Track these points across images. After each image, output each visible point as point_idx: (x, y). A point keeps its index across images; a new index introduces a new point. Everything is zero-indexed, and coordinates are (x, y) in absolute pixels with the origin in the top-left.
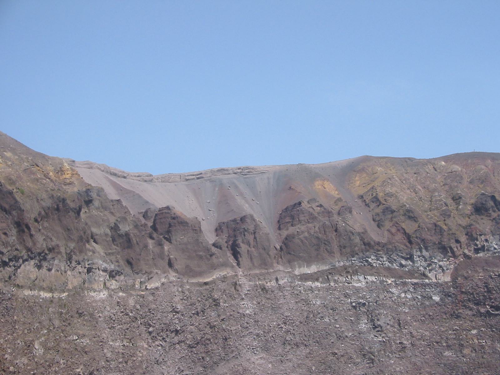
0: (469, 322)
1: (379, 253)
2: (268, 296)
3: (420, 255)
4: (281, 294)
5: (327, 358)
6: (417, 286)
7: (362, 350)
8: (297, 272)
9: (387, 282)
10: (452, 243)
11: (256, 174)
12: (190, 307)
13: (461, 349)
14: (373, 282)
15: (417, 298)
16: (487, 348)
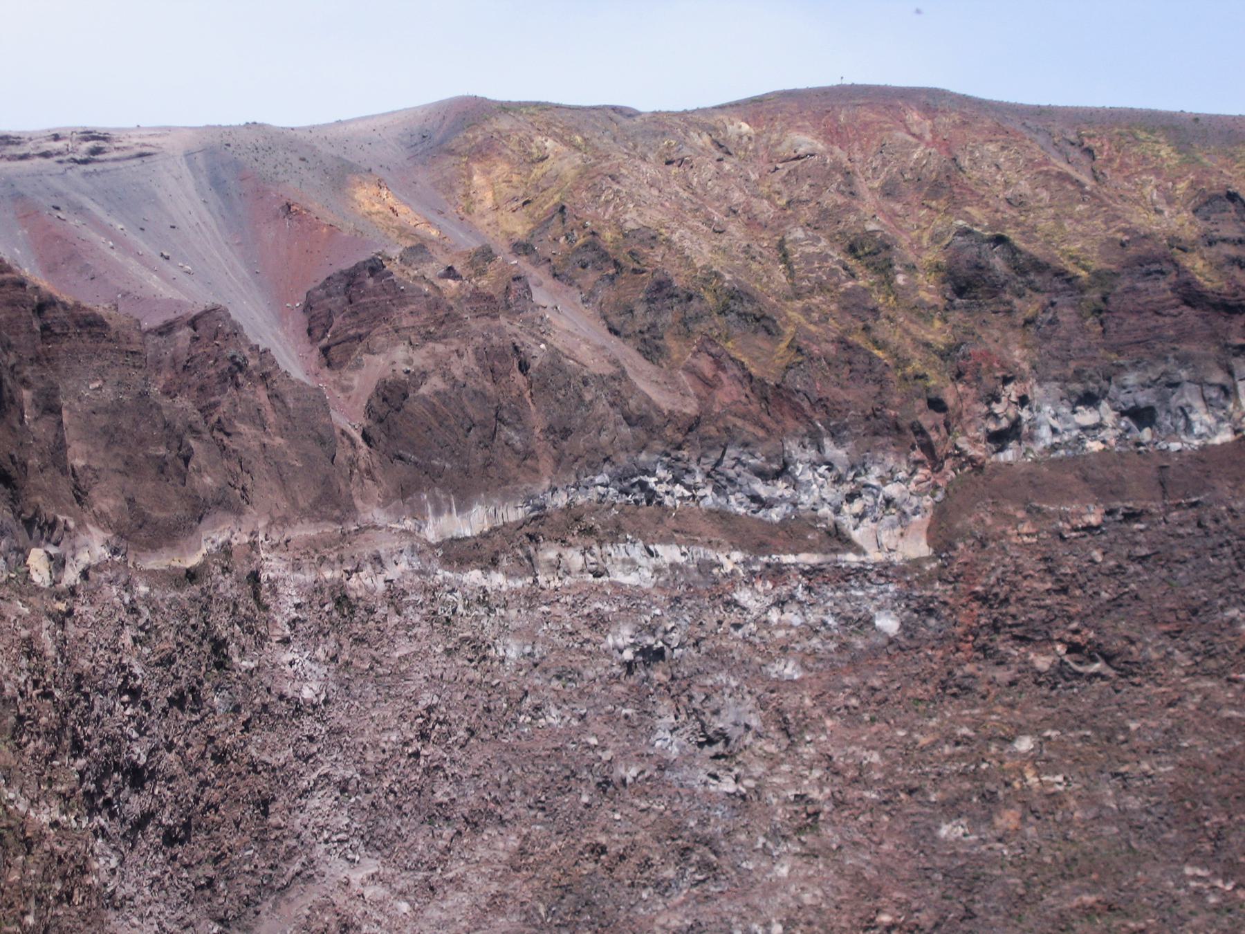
0: (1000, 709)
1: (680, 454)
2: (357, 628)
3: (814, 459)
4: (396, 620)
5: (577, 868)
6: (821, 581)
7: (676, 830)
8: (431, 534)
9: (720, 566)
10: (921, 412)
11: (115, 160)
12: (159, 670)
13: (990, 812)
14: (674, 566)
15: (824, 623)
16: (1072, 802)
